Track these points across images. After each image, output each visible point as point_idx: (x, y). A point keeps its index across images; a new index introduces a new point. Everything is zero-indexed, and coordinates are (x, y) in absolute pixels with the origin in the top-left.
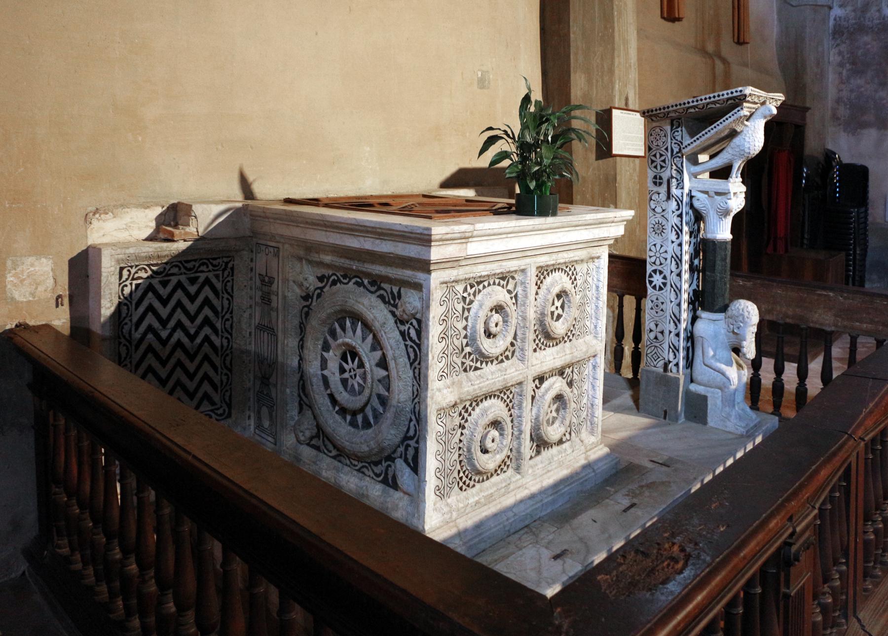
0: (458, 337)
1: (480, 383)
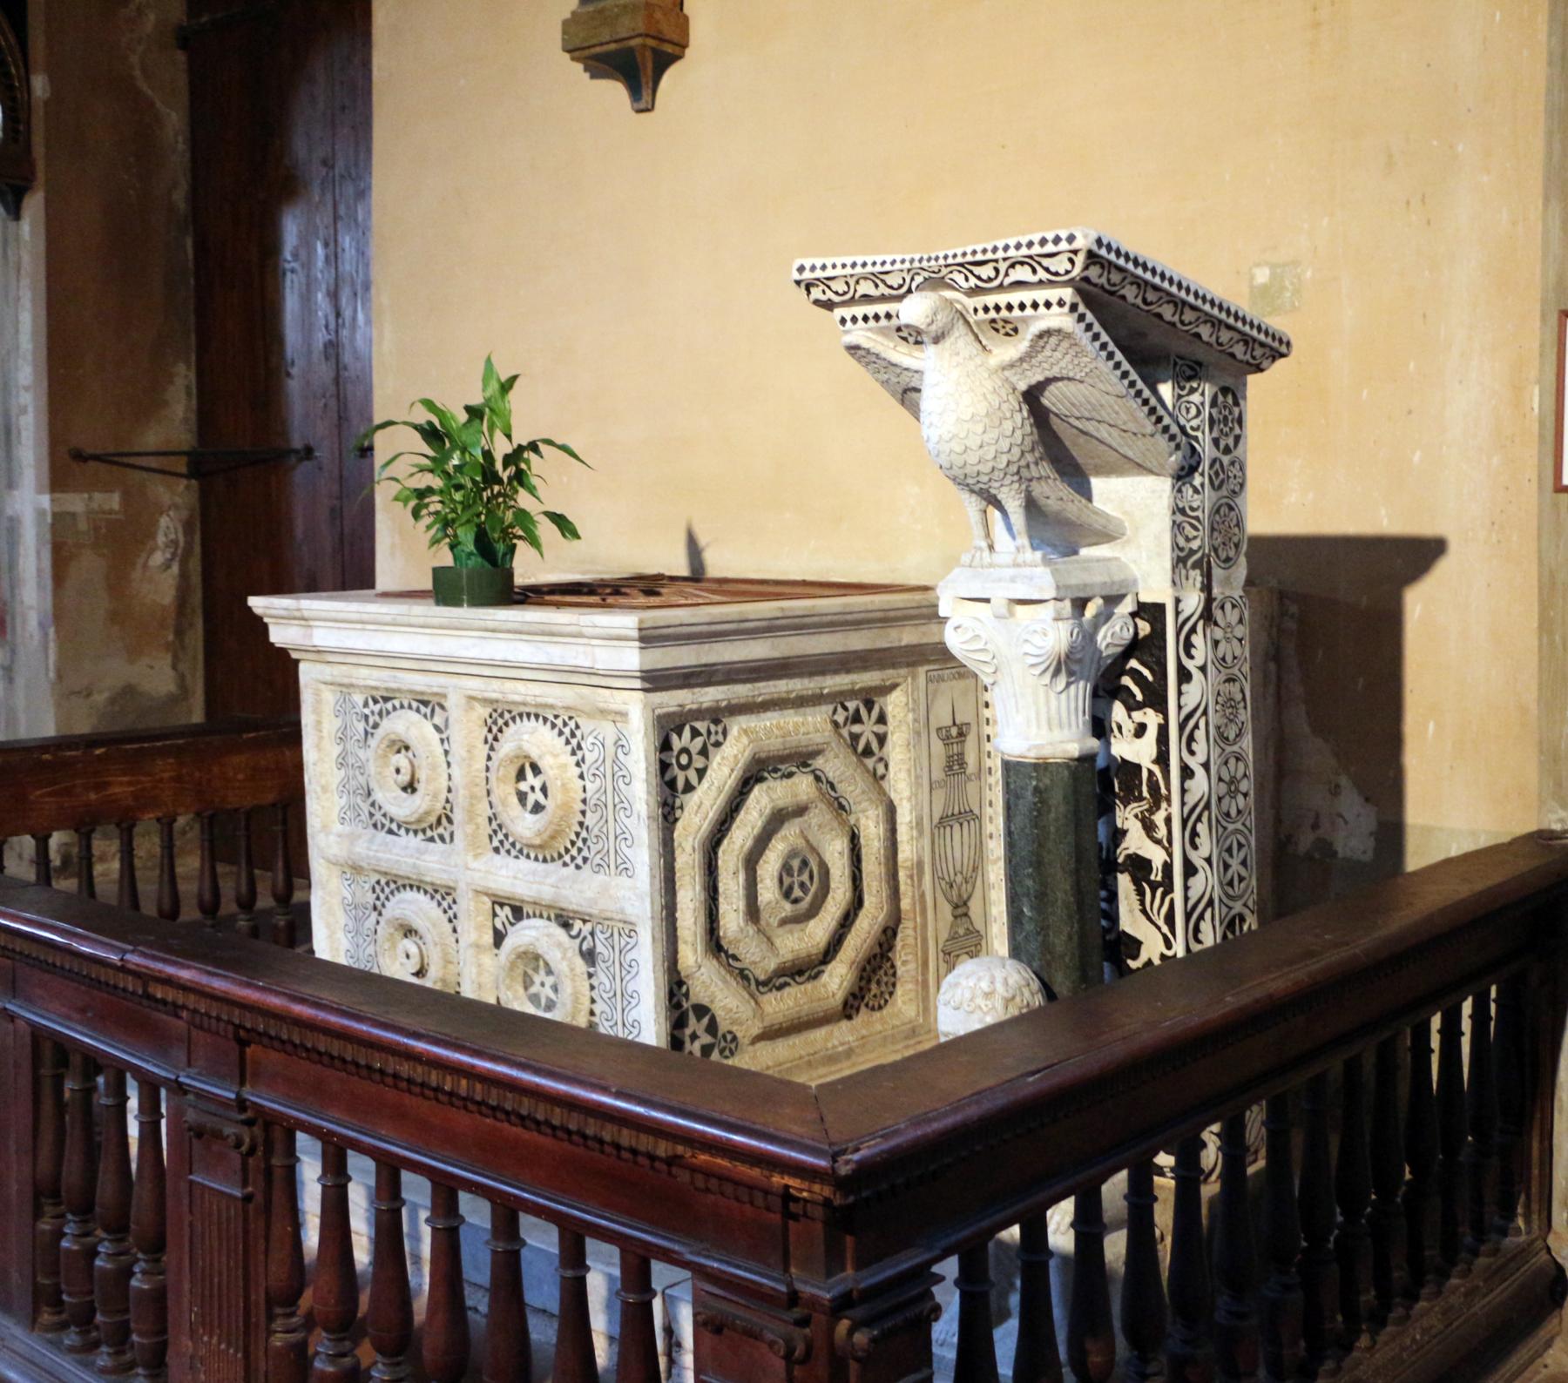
1: (377, 851)
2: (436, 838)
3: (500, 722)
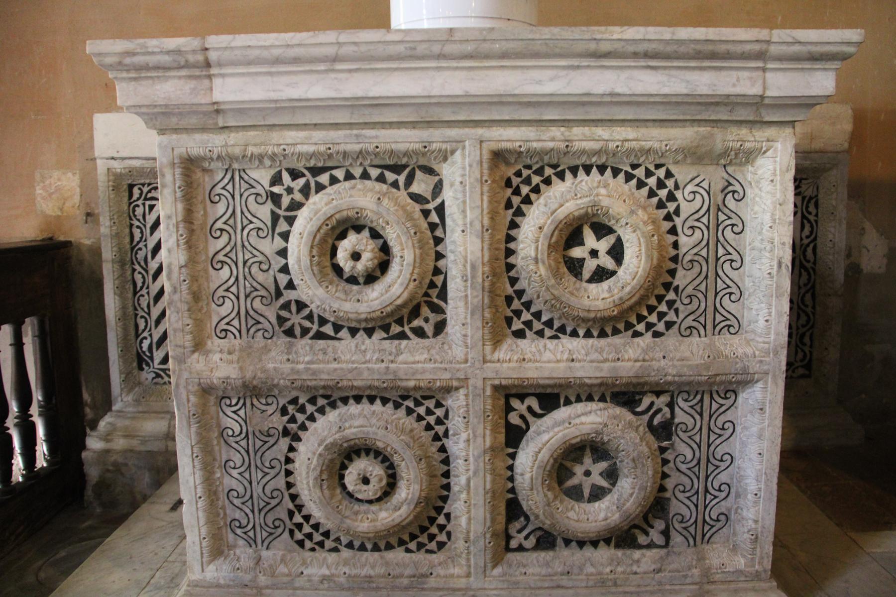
0: (265, 267)
2: (409, 333)
3: (536, 180)
